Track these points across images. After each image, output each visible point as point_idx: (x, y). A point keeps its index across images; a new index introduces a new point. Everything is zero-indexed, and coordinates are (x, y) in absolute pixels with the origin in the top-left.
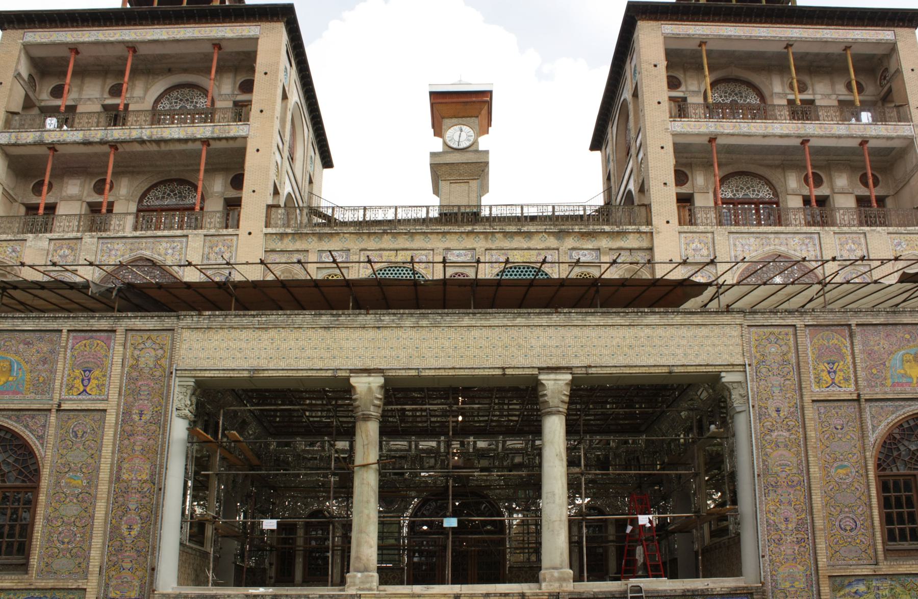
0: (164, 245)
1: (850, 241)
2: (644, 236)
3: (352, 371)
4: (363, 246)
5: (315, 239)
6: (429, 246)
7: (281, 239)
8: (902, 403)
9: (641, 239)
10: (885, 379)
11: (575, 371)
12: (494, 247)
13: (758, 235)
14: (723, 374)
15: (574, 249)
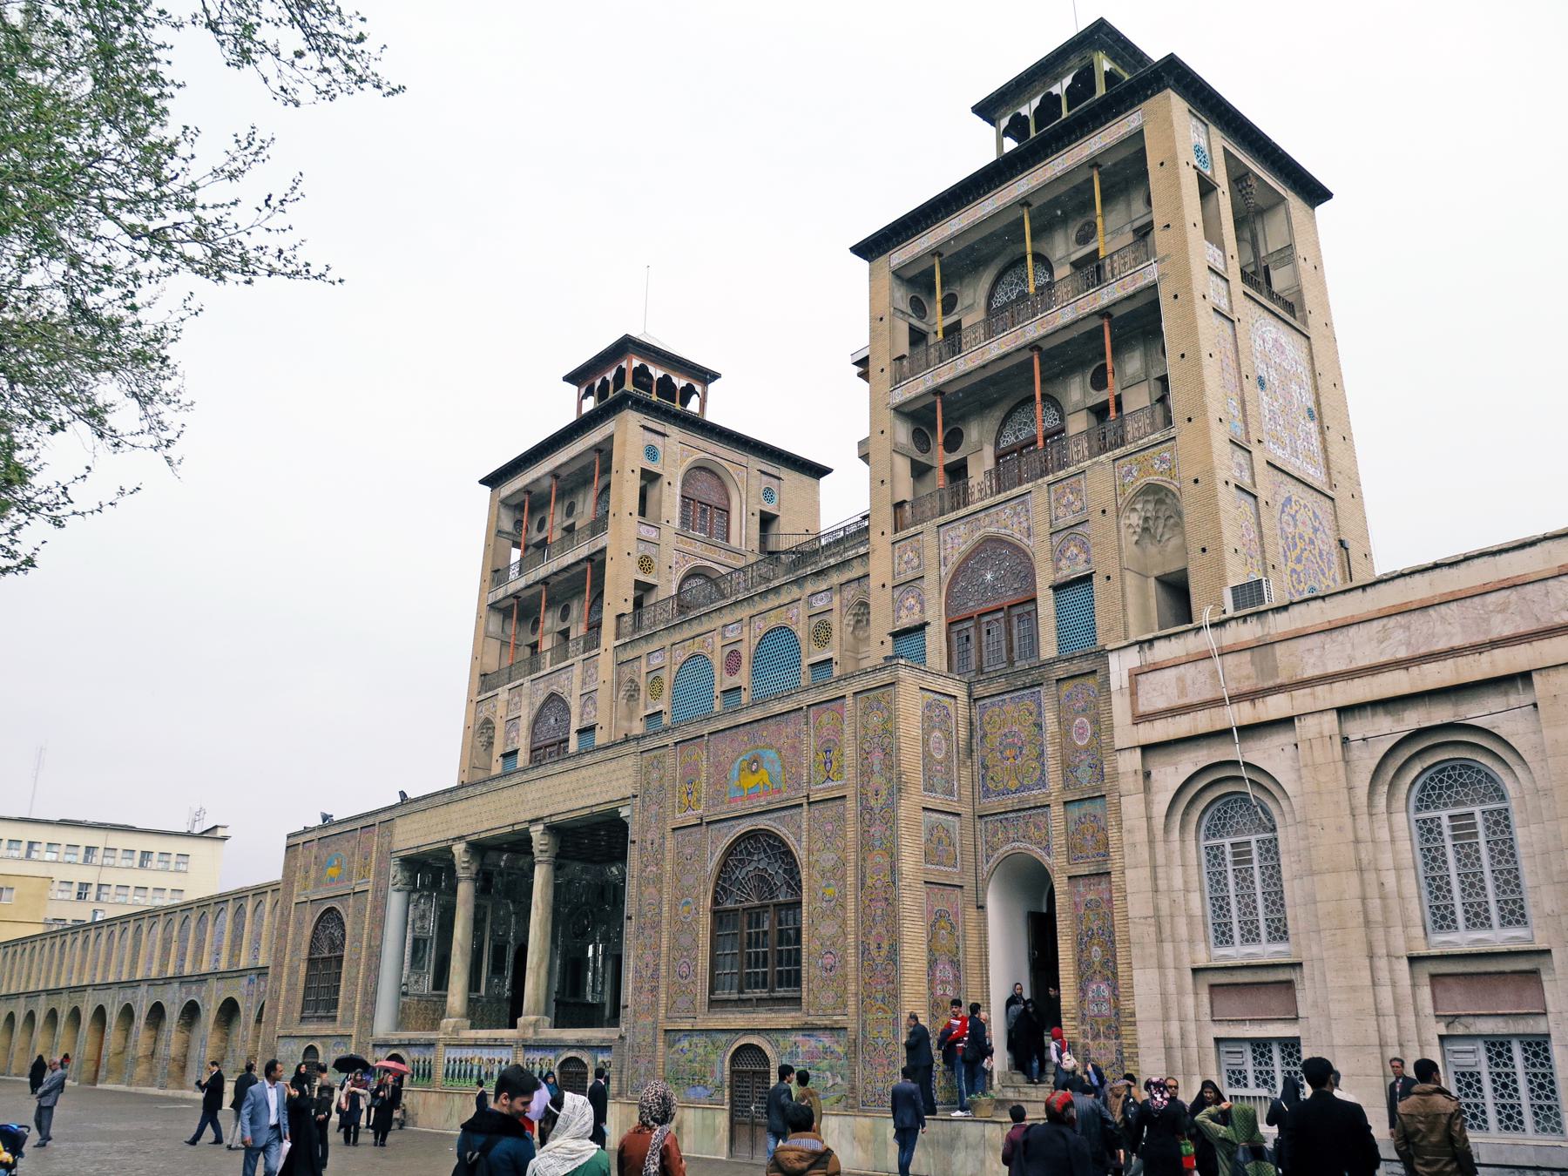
0: (564, 676)
1: (1068, 490)
2: (865, 558)
3: (454, 840)
4: (672, 641)
5: (643, 642)
6: (713, 627)
8: (733, 822)
11: (547, 820)
12: (755, 613)
14: (620, 810)
15: (812, 595)
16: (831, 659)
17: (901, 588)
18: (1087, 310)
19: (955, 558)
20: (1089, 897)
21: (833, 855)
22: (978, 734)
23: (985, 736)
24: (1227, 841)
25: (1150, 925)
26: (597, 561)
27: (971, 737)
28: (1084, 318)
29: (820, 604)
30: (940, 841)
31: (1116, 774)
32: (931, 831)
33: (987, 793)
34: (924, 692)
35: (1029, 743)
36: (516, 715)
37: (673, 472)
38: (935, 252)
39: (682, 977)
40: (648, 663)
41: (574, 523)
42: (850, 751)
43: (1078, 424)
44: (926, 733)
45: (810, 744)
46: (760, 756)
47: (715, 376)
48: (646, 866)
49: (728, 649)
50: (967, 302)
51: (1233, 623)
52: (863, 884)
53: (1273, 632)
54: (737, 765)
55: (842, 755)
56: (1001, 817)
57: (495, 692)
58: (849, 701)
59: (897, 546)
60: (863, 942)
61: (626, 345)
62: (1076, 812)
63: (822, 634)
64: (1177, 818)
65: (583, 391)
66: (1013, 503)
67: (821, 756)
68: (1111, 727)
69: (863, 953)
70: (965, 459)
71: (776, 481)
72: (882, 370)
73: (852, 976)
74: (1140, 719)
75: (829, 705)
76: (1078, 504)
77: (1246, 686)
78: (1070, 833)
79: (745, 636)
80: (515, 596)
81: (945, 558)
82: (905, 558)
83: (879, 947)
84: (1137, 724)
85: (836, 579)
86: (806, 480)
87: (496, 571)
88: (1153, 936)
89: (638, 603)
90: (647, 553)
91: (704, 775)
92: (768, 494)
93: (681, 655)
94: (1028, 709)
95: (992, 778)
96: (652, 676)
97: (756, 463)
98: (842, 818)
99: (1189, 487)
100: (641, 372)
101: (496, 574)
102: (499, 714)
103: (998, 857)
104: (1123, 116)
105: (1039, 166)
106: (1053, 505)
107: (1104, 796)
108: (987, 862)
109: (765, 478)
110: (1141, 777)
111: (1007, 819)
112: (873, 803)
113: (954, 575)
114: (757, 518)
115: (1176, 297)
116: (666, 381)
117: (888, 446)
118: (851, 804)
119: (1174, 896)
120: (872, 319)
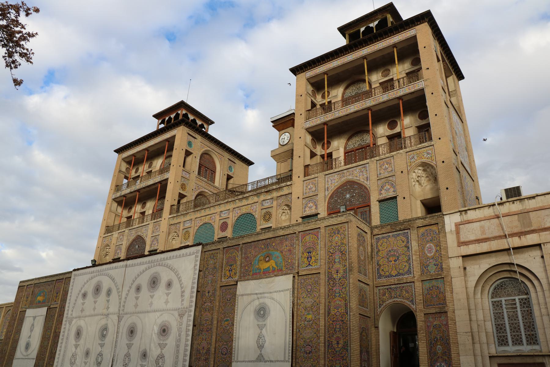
1: (385, 163)
2: (289, 187)
4: (196, 217)
6: (215, 212)
7: (173, 219)
9: (289, 189)
10: (250, 272)
13: (339, 173)
16: (271, 227)
17: (307, 199)
18: (394, 96)
19: (332, 188)
20: (435, 323)
21: (311, 300)
22: (376, 250)
23: (379, 251)
24: (503, 299)
25: (469, 336)
26: (164, 184)
27: (372, 252)
28: (392, 99)
29: (266, 205)
30: (363, 295)
31: (449, 268)
32: (361, 290)
33: (380, 276)
34: (358, 228)
35: (403, 254)
36: (121, 244)
37: (197, 153)
38: (325, 73)
39: (223, 354)
40: (184, 225)
41: (152, 170)
42: (321, 253)
43: (382, 141)
44: (359, 247)
45: (299, 250)
46: (271, 254)
47: (212, 123)
48: (205, 303)
49: (222, 221)
50: (334, 95)
51: (508, 204)
52: (329, 313)
53: (528, 208)
54: (257, 258)
55: (317, 254)
56: (388, 287)
57: (112, 234)
58: (322, 230)
59: (305, 182)
60: (328, 340)
61: (182, 105)
62: (427, 285)
63: (267, 216)
64: (480, 288)
65: (160, 121)
66: (359, 167)
67: (306, 255)
68: (446, 248)
69: (328, 346)
70: (332, 153)
71: (233, 164)
72: (301, 114)
73: (322, 356)
74: (461, 244)
75: (312, 231)
76: (390, 169)
77: (516, 230)
78: (425, 295)
79: (231, 216)
80: (124, 196)
81: (328, 188)
82: (309, 187)
83: (338, 343)
84: (460, 246)
85: (275, 194)
86: (245, 165)
87: (117, 186)
88: (471, 341)
89: (179, 202)
90: (185, 183)
91: (239, 263)
92: (230, 168)
93: (199, 223)
94: (401, 240)
95: (383, 270)
96: (185, 230)
97: (227, 155)
98: (317, 283)
99: (440, 164)
100: (185, 116)
101: (118, 188)
102: (112, 243)
103: (386, 305)
104: (408, 30)
105: (372, 45)
106: (379, 168)
107: (443, 278)
108: (380, 307)
109: (230, 162)
110: (462, 269)
111: (391, 288)
112: (335, 276)
113: (331, 195)
114: (226, 177)
115: (432, 93)
116: (194, 121)
117: (303, 144)
118: (322, 276)
119: (479, 323)
120: (297, 95)
